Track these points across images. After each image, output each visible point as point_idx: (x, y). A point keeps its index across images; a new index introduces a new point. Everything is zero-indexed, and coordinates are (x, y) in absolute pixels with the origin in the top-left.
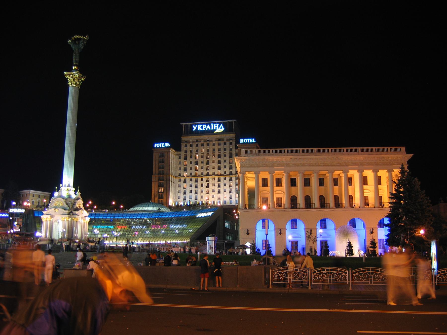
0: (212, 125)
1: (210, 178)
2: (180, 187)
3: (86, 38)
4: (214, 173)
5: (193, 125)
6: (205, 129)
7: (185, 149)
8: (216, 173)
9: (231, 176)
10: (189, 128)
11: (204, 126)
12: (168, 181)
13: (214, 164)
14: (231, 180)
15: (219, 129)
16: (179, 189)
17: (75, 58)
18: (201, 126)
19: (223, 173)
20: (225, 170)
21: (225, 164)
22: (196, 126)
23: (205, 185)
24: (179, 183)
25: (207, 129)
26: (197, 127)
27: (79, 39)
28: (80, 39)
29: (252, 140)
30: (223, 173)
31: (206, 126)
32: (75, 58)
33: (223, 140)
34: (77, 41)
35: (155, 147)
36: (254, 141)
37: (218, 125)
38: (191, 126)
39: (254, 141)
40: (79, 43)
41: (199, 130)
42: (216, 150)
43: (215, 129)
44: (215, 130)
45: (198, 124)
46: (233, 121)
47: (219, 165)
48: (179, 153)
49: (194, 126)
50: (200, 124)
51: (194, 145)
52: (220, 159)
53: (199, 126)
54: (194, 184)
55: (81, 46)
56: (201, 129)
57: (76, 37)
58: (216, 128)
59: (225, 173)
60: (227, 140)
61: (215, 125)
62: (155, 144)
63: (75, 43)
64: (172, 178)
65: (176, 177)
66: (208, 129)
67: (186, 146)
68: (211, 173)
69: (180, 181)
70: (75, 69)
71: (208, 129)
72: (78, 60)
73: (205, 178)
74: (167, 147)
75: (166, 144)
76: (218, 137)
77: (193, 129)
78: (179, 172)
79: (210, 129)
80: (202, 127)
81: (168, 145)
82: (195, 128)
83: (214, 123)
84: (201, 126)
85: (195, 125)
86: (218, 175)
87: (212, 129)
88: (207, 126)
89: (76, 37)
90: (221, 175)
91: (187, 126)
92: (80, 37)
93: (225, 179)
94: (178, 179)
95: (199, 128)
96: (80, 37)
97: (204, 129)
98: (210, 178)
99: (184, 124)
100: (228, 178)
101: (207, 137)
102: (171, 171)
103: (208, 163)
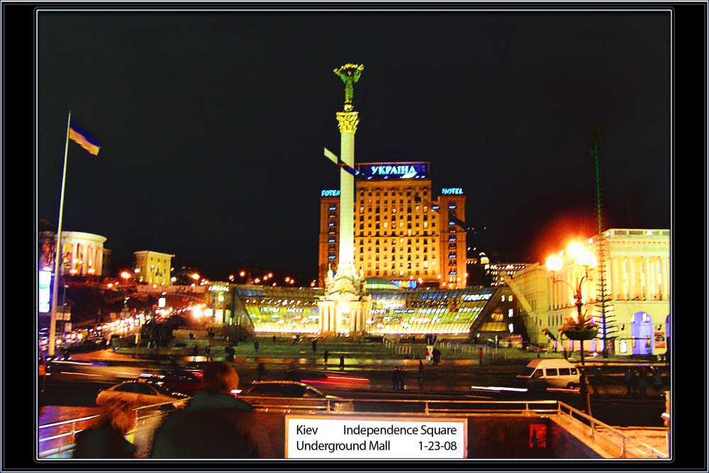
3: (361, 68)
5: (373, 165)
7: (362, 198)
8: (405, 234)
9: (426, 238)
11: (388, 169)
14: (425, 242)
15: (409, 173)
17: (349, 94)
19: (414, 234)
20: (418, 229)
21: (418, 221)
25: (391, 173)
27: (353, 70)
29: (459, 191)
30: (414, 234)
31: (391, 167)
32: (349, 94)
33: (414, 189)
34: (351, 72)
36: (461, 192)
37: (407, 167)
39: (461, 192)
40: (352, 75)
41: (380, 173)
43: (402, 173)
44: (403, 175)
45: (379, 166)
46: (429, 163)
47: (409, 222)
49: (373, 168)
50: (383, 165)
51: (374, 194)
52: (410, 214)
55: (357, 78)
56: (384, 173)
57: (348, 66)
59: (418, 233)
60: (420, 189)
67: (362, 194)
72: (352, 96)
73: (390, 240)
76: (408, 184)
77: (372, 172)
80: (385, 170)
82: (374, 170)
85: (376, 166)
86: (407, 236)
87: (399, 173)
89: (348, 66)
90: (412, 236)
93: (418, 241)
95: (381, 171)
100: (422, 241)
101: (391, 184)
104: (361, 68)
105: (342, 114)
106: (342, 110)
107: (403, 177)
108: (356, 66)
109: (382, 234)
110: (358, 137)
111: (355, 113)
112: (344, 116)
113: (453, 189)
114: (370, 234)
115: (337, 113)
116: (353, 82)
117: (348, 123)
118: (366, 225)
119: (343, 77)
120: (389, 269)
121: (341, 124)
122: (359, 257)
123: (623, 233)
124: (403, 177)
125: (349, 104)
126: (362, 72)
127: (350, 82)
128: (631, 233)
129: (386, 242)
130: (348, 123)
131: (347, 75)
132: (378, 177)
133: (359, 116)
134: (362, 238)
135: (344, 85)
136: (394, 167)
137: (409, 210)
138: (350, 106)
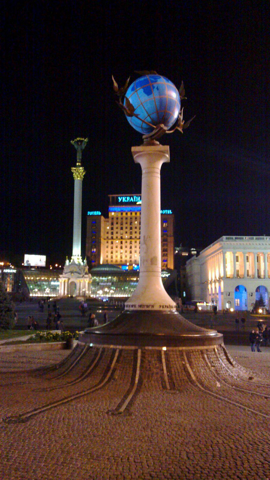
0: (135, 197)
1: (133, 241)
2: (107, 247)
3: (86, 140)
4: (136, 237)
5: (119, 196)
6: (129, 200)
10: (115, 199)
12: (100, 243)
13: (136, 230)
16: (107, 249)
17: (79, 156)
18: (125, 198)
22: (121, 198)
23: (129, 246)
24: (107, 244)
25: (130, 201)
26: (122, 199)
27: (81, 141)
28: (82, 141)
32: (79, 156)
35: (88, 214)
36: (171, 213)
38: (117, 197)
39: (171, 213)
41: (123, 201)
42: (137, 218)
43: (137, 201)
44: (137, 202)
45: (122, 197)
48: (107, 220)
49: (119, 198)
53: (123, 198)
54: (110, 245)
55: (83, 147)
56: (126, 201)
57: (78, 139)
58: (138, 200)
61: (137, 197)
62: (88, 212)
63: (78, 144)
64: (102, 240)
65: (105, 239)
66: (131, 201)
68: (133, 237)
69: (107, 242)
70: (79, 165)
71: (131, 201)
72: (81, 158)
74: (99, 215)
75: (98, 212)
78: (107, 235)
79: (133, 201)
80: (126, 199)
81: (99, 213)
82: (120, 199)
83: (136, 196)
84: (125, 198)
87: (135, 201)
88: (130, 198)
89: (78, 139)
91: (113, 198)
92: (82, 139)
94: (106, 241)
95: (124, 200)
96: (82, 139)
97: (128, 201)
98: (133, 241)
99: (111, 196)
102: (102, 234)
103: (131, 228)
104: (86, 140)
105: (75, 168)
106: (75, 166)
107: (137, 203)
108: (83, 139)
109: (114, 237)
110: (85, 182)
111: (81, 168)
112: (75, 170)
113: (166, 211)
114: (117, 237)
115: (72, 168)
116: (82, 149)
117: (78, 173)
118: (115, 233)
119: (76, 146)
120: (109, 259)
121: (74, 174)
122: (110, 252)
123: (253, 239)
124: (137, 203)
125: (79, 162)
126: (87, 143)
127: (79, 149)
128: (256, 239)
129: (126, 242)
130: (78, 173)
131: (78, 144)
132: (122, 203)
133: (85, 169)
134: (112, 240)
135: (75, 151)
136: (132, 198)
137: (131, 223)
138: (80, 164)
